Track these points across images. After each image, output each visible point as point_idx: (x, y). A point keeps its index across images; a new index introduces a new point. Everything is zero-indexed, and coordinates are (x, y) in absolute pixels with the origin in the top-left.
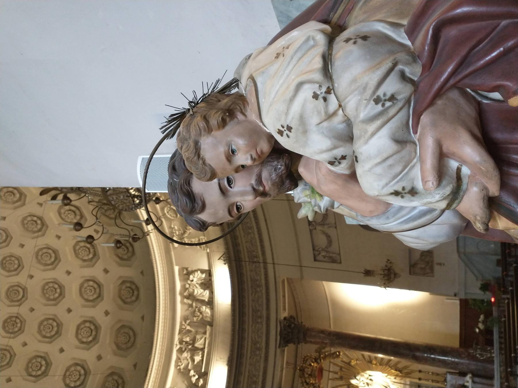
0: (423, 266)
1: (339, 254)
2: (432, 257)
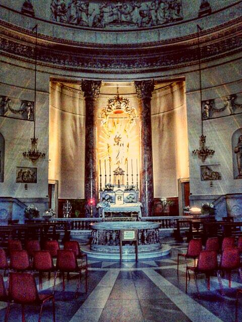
0: (208, 174)
1: (209, 119)
2: (216, 179)
